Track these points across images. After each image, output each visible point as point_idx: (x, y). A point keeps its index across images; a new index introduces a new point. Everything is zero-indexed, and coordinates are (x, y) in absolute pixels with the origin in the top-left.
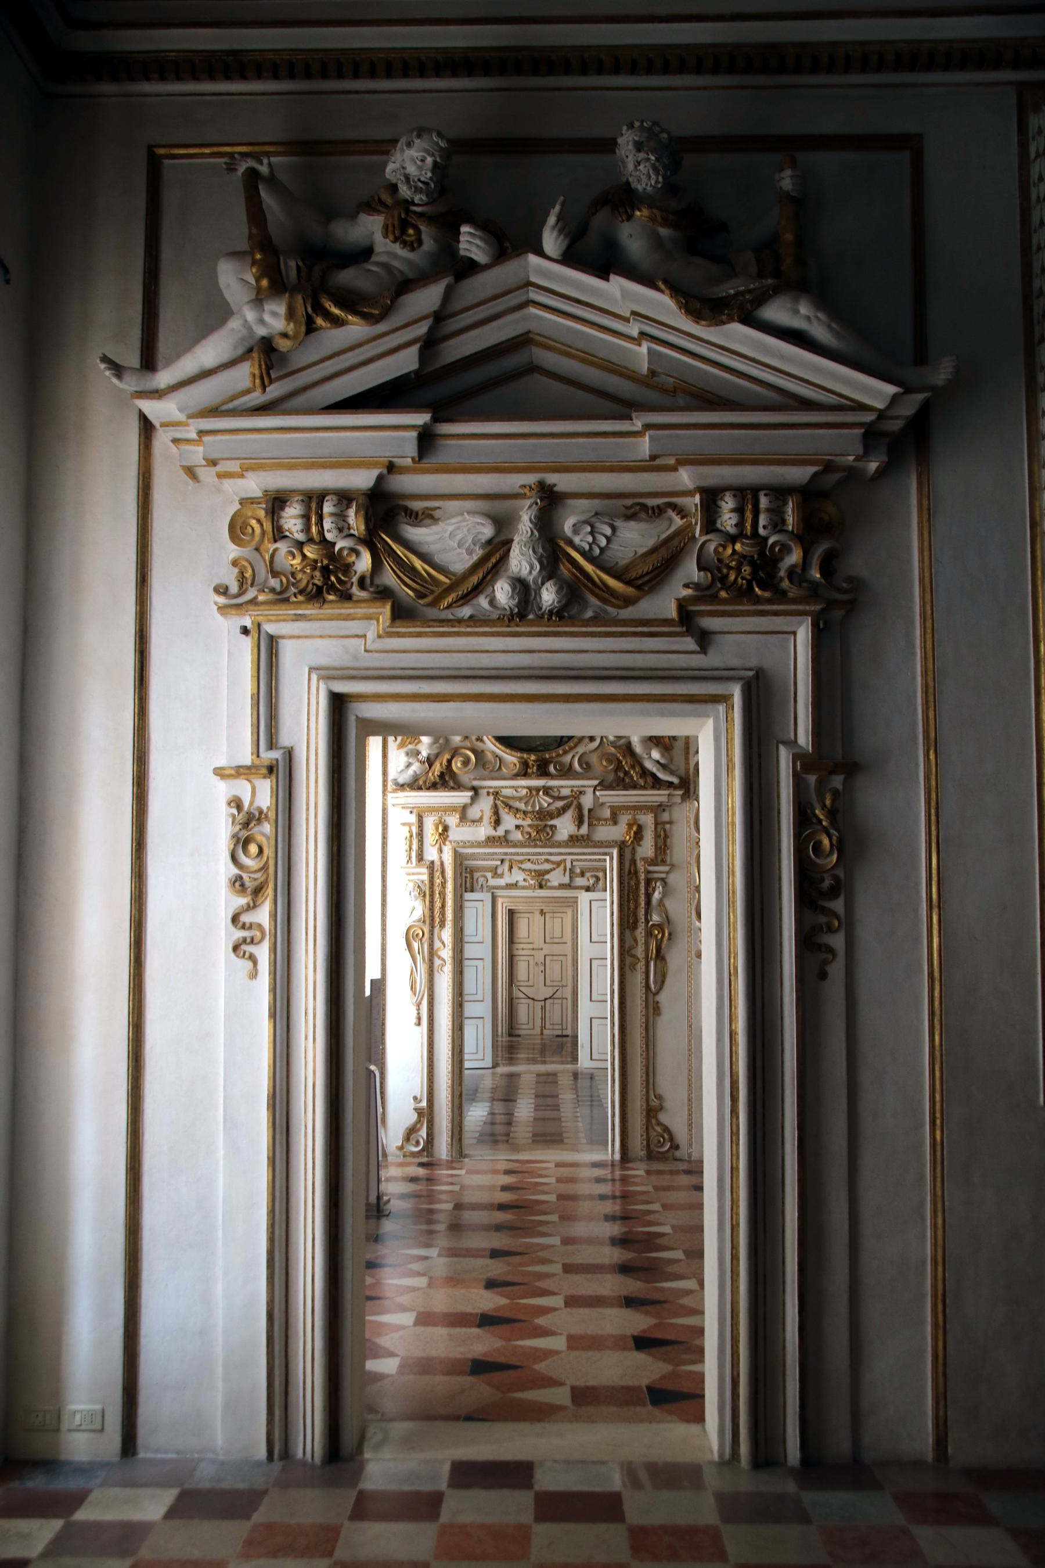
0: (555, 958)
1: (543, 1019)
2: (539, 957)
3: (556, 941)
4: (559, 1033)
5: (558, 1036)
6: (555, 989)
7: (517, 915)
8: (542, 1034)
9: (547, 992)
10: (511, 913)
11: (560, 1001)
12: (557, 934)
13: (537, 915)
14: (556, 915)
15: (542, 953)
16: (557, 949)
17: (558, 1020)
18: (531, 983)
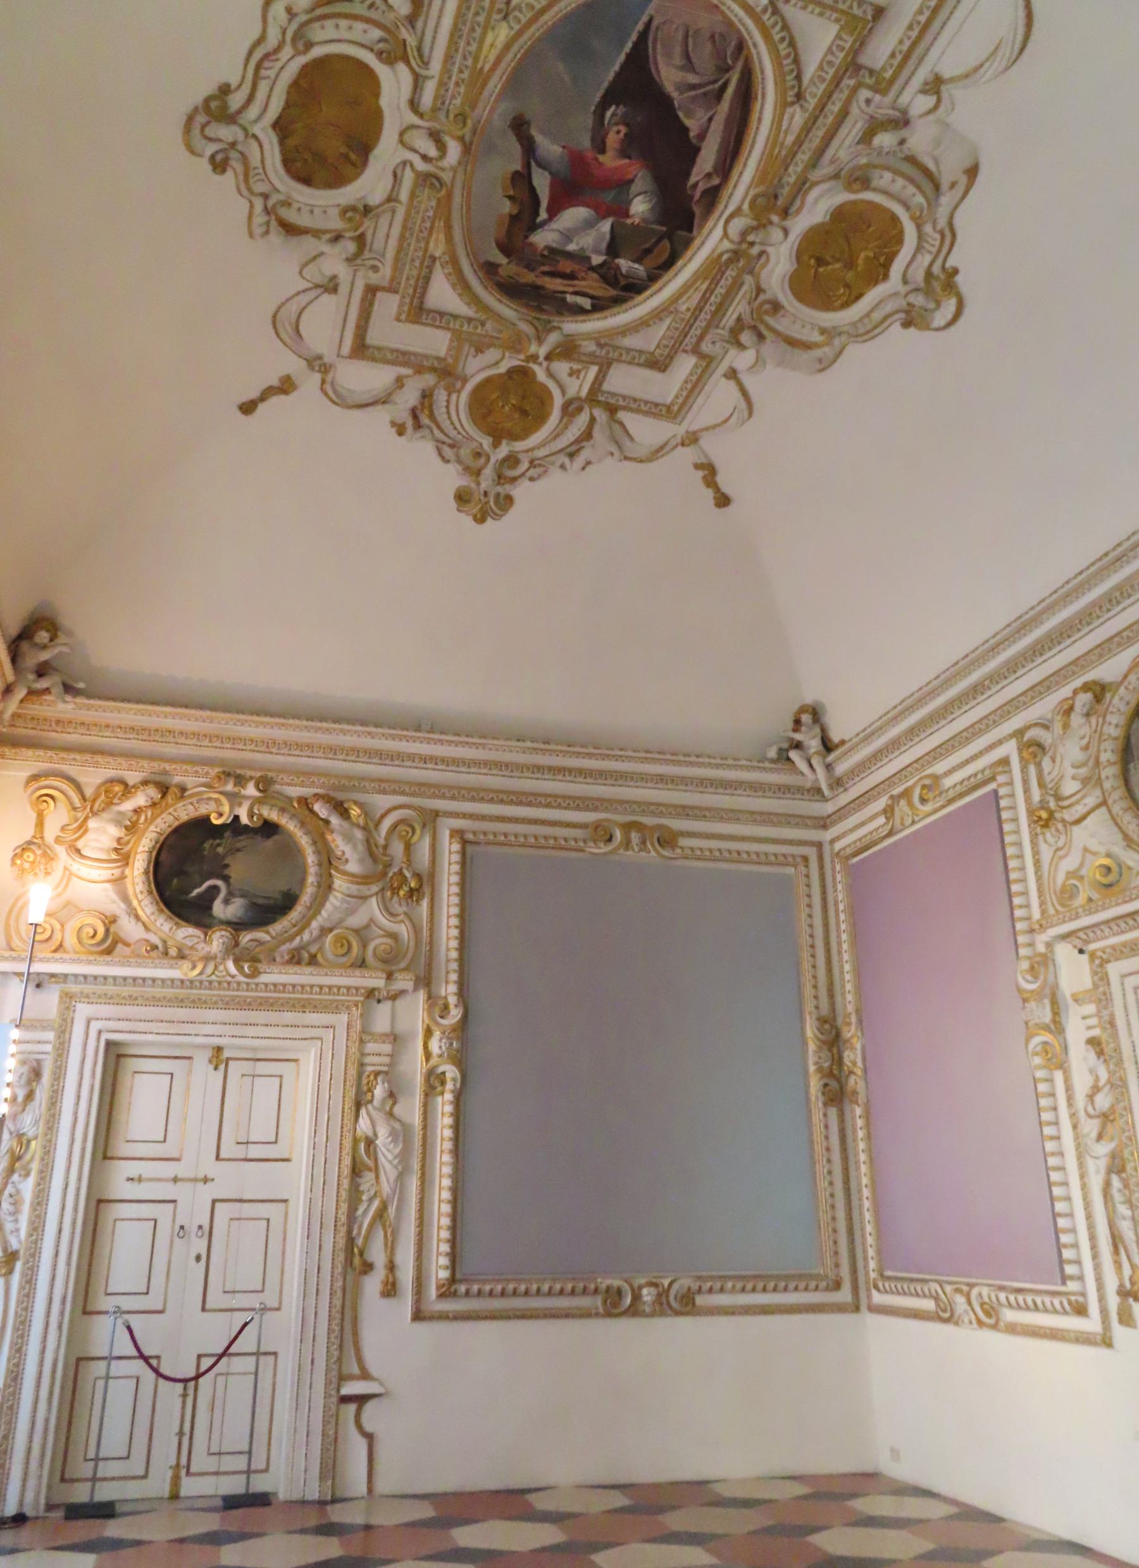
0: (248, 1210)
1: (186, 1435)
2: (194, 1205)
3: (255, 1152)
4: (234, 1486)
5: (231, 1503)
6: (240, 1318)
7: (132, 1064)
8: (175, 1496)
9: (212, 1333)
10: (115, 1056)
11: (249, 1363)
12: (262, 1129)
13: (201, 1061)
14: (262, 1068)
15: (206, 1193)
16: (253, 1180)
17: (235, 1436)
18: (152, 1302)
